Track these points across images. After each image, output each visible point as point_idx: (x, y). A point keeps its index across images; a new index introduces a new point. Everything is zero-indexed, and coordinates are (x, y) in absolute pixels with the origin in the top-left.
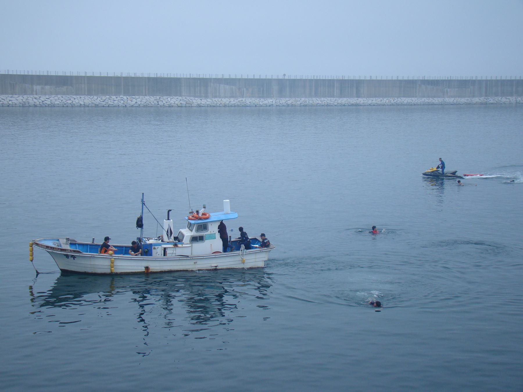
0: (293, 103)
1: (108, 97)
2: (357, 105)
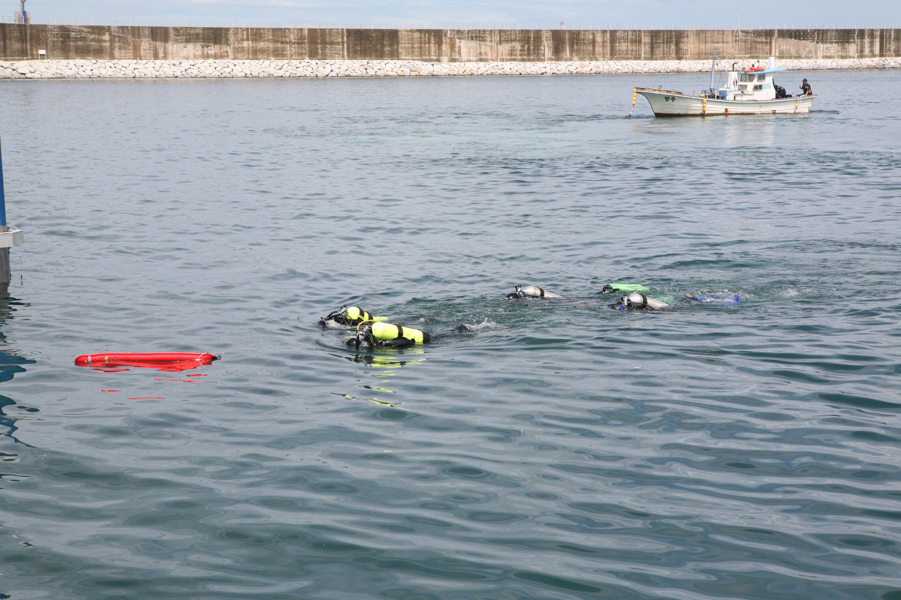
0: (578, 70)
1: (287, 61)
2: (679, 72)
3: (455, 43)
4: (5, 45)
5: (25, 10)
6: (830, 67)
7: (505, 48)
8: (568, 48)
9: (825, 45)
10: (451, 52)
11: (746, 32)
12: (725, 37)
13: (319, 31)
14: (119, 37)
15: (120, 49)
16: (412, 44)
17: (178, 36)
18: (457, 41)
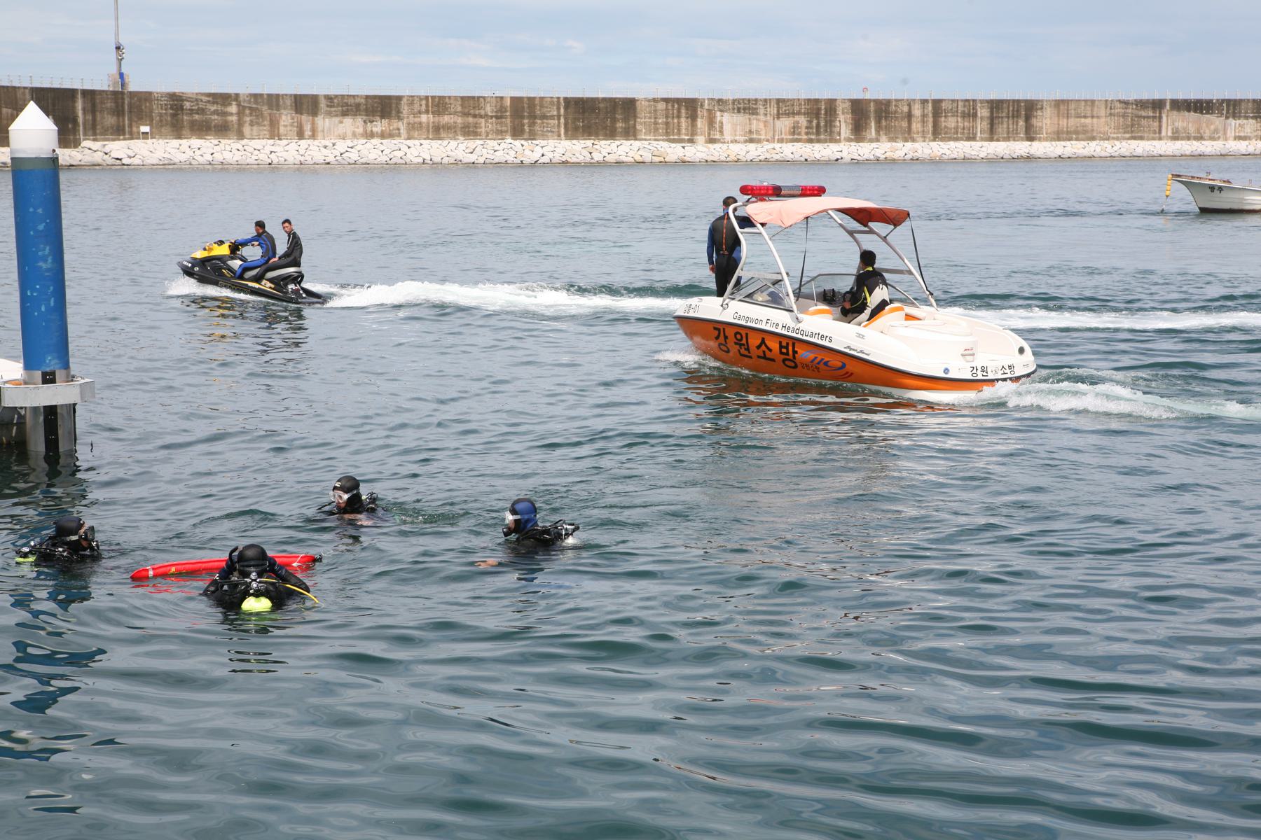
0: (887, 155)
1: (481, 142)
2: (1029, 158)
3: (715, 117)
4: (94, 120)
5: (123, 71)
6: (1244, 152)
7: (785, 124)
8: (873, 124)
9: (1238, 122)
10: (709, 129)
11: (1126, 103)
12: (1096, 109)
13: (525, 100)
14: (250, 108)
15: (251, 125)
16: (656, 118)
17: (331, 106)
18: (718, 114)
